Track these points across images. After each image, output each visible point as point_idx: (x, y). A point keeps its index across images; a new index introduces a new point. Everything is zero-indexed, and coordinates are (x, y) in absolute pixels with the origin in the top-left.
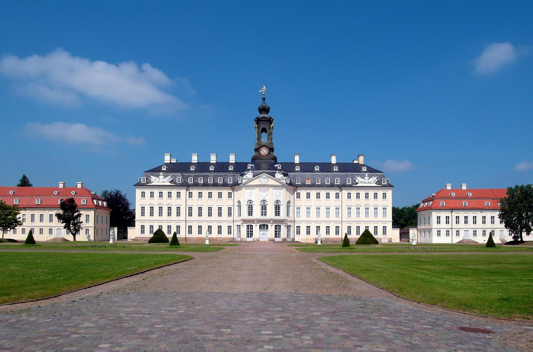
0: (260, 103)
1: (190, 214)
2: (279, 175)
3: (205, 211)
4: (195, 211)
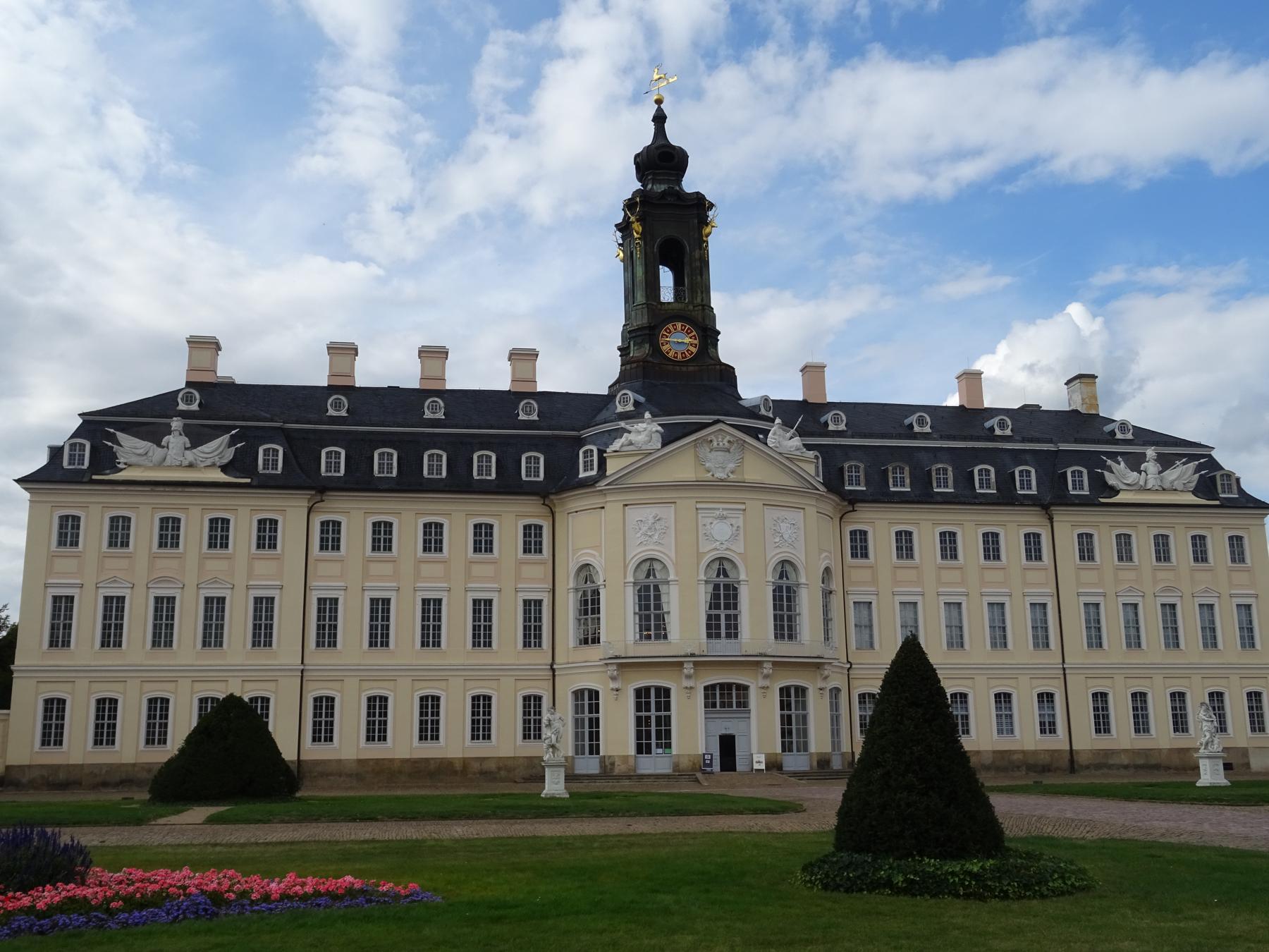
0: (646, 137)
1: (327, 635)
2: (782, 439)
3: (405, 623)
4: (353, 623)
